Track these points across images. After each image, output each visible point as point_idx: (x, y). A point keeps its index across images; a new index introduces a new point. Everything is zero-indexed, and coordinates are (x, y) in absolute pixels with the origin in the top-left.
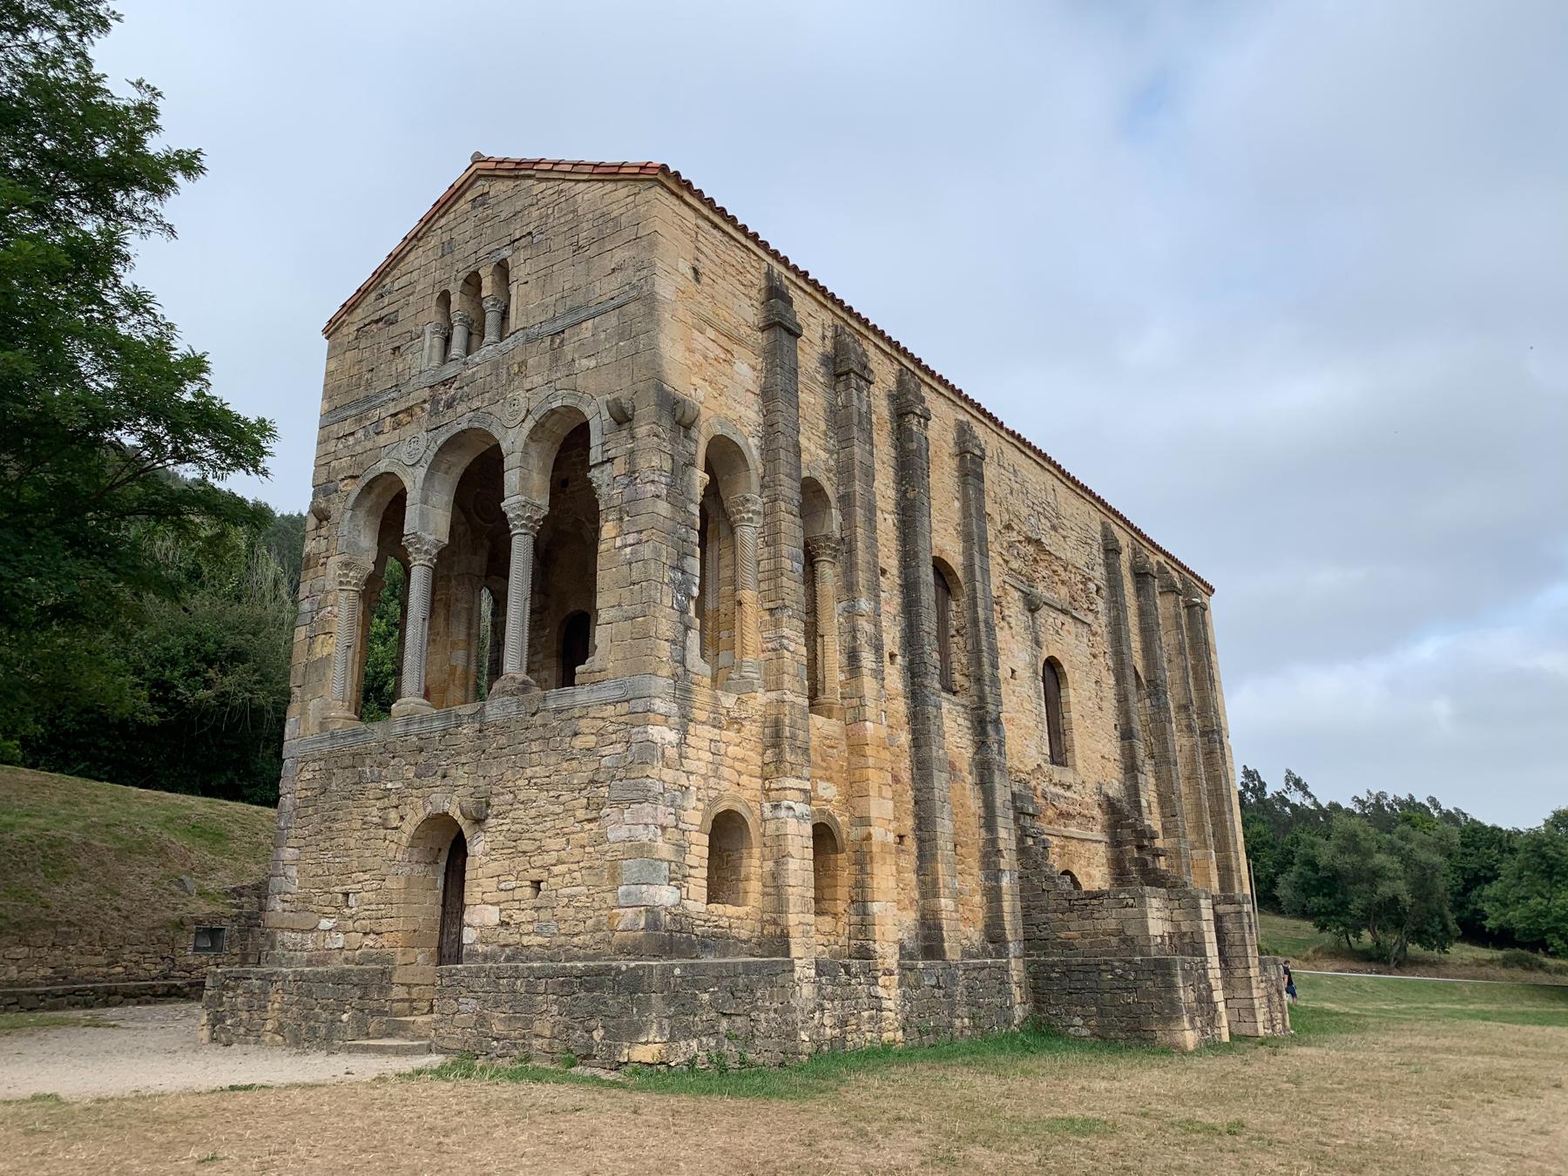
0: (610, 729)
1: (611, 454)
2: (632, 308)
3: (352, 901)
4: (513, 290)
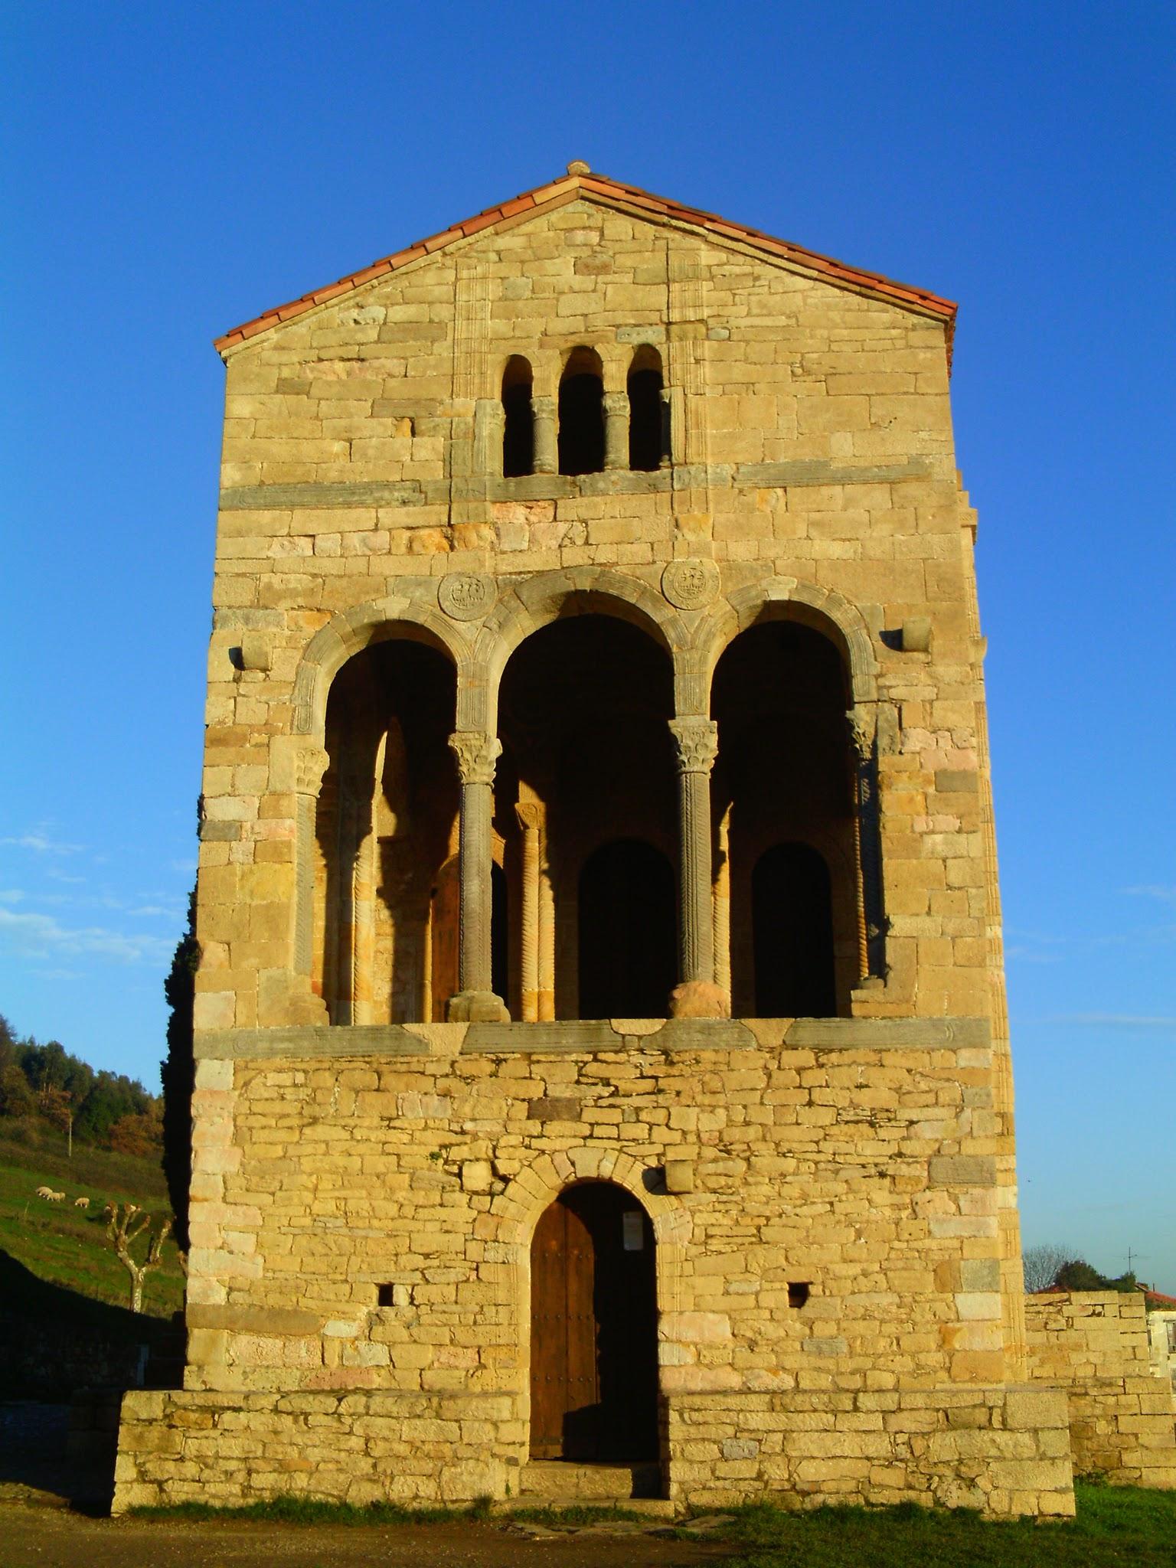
0: (923, 1086)
1: (895, 693)
2: (912, 489)
3: (400, 1296)
4: (672, 394)
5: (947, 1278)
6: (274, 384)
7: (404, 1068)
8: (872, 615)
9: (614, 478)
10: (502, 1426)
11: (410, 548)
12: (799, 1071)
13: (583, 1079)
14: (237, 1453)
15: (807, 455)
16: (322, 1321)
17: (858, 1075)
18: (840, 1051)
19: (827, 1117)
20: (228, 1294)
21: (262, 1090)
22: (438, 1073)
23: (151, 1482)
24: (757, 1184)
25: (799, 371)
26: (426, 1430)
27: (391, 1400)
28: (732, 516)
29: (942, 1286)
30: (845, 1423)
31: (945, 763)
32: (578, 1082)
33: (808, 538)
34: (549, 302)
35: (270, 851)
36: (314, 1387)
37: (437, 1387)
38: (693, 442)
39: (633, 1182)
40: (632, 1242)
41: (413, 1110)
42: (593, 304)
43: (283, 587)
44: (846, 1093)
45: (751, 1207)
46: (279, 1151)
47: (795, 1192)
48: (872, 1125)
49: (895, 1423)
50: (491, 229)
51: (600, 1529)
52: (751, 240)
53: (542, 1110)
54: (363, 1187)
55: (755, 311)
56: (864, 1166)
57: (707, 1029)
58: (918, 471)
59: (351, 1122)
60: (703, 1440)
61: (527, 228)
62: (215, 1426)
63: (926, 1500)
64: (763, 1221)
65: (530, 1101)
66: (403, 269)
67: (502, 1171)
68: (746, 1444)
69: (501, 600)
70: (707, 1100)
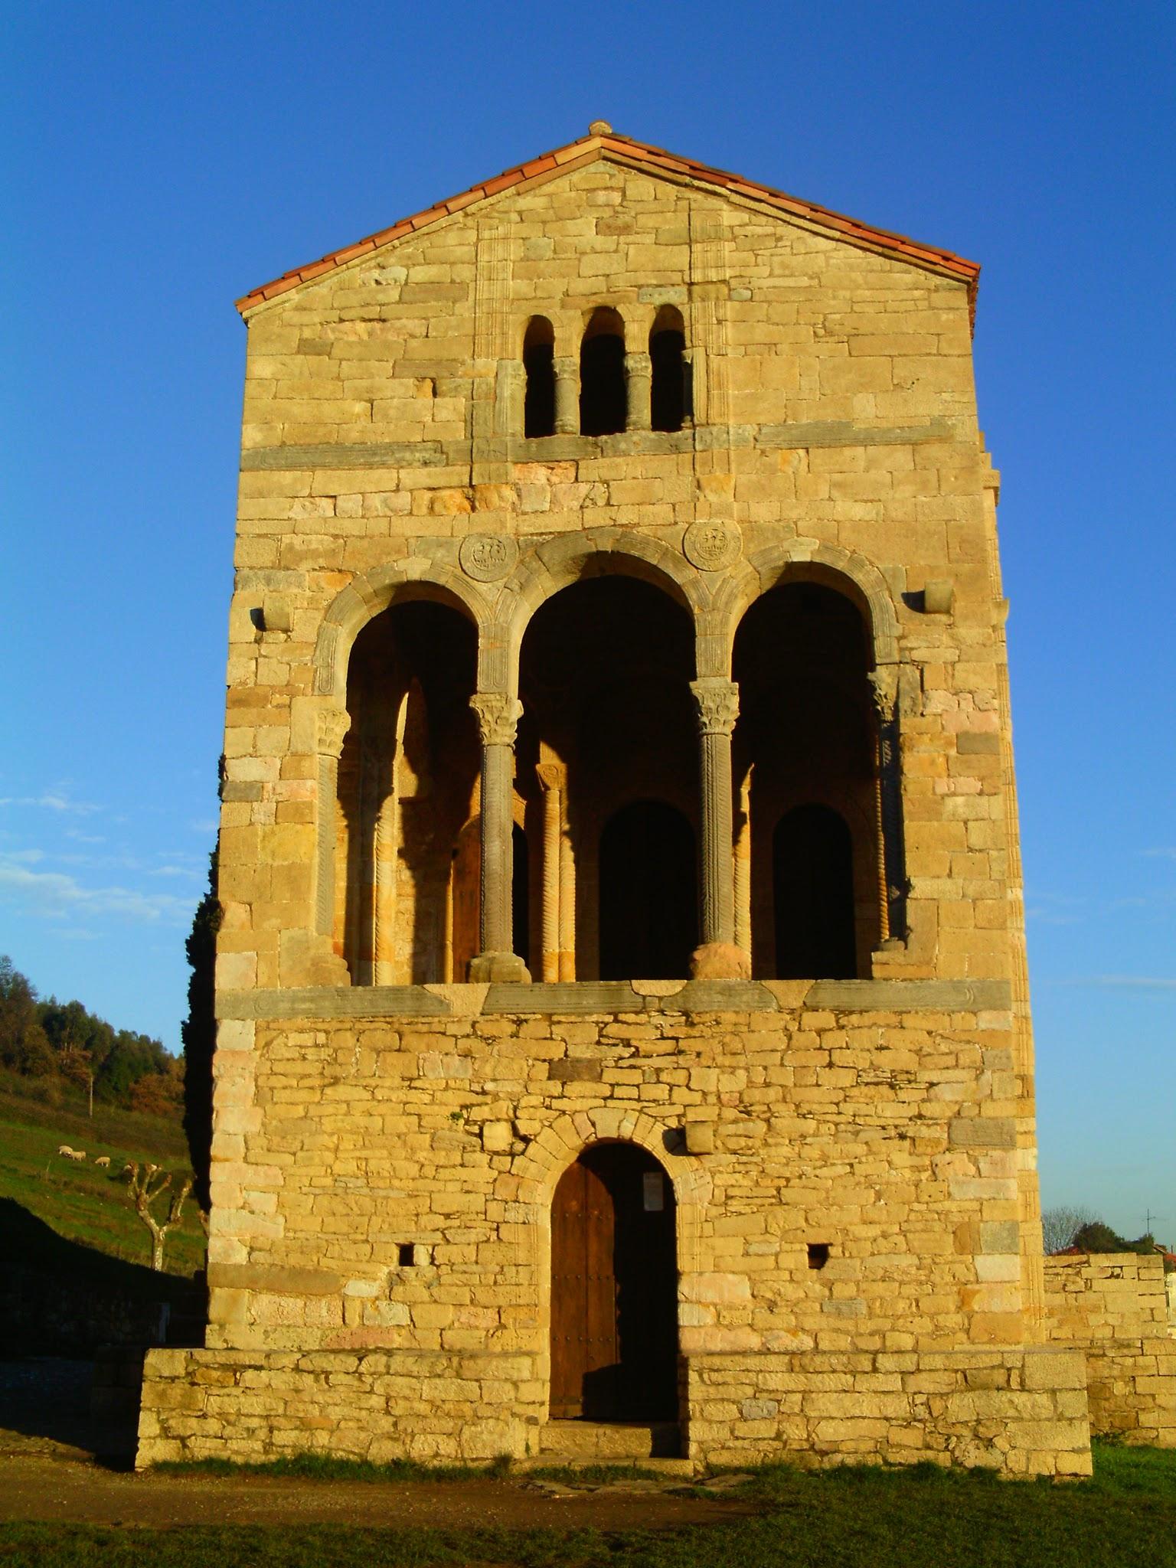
0: (944, 1048)
1: (916, 655)
2: (935, 451)
3: (421, 1255)
4: (695, 355)
5: (966, 1240)
6: (295, 345)
7: (425, 1028)
8: (894, 577)
9: (635, 438)
10: (522, 1386)
11: (431, 509)
12: (820, 1032)
13: (603, 1040)
14: (258, 1411)
15: (829, 416)
16: (343, 1281)
17: (878, 1036)
18: (861, 1012)
19: (847, 1079)
20: (249, 1254)
21: (284, 1050)
22: (459, 1033)
23: (174, 1438)
24: (776, 1145)
25: (821, 332)
26: (447, 1389)
27: (411, 1360)
28: (754, 477)
29: (961, 1248)
30: (864, 1383)
31: (967, 726)
32: (598, 1043)
33: (830, 499)
34: (571, 263)
35: (292, 812)
36: (335, 1346)
37: (458, 1346)
38: (715, 402)
39: (653, 1143)
40: (652, 1203)
41: (433, 1070)
42: (615, 265)
43: (304, 548)
44: (866, 1055)
45: (770, 1168)
46: (300, 1111)
47: (815, 1153)
48: (892, 1086)
49: (913, 1383)
50: (512, 190)
51: (619, 1487)
52: (773, 200)
53: (563, 1070)
54: (384, 1147)
55: (777, 272)
56: (884, 1128)
57: (728, 991)
58: (940, 432)
59: (373, 1082)
60: (723, 1400)
61: (548, 188)
62: (237, 1383)
63: (944, 1460)
64: (783, 1182)
65: (550, 1061)
66: (425, 230)
67: (523, 1132)
68: (766, 1404)
69: (522, 562)
70: (728, 1061)
